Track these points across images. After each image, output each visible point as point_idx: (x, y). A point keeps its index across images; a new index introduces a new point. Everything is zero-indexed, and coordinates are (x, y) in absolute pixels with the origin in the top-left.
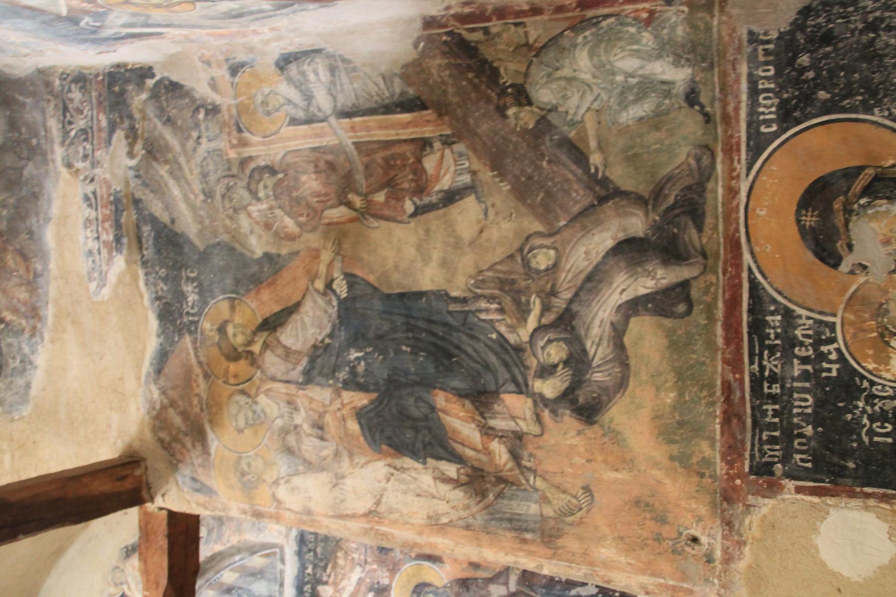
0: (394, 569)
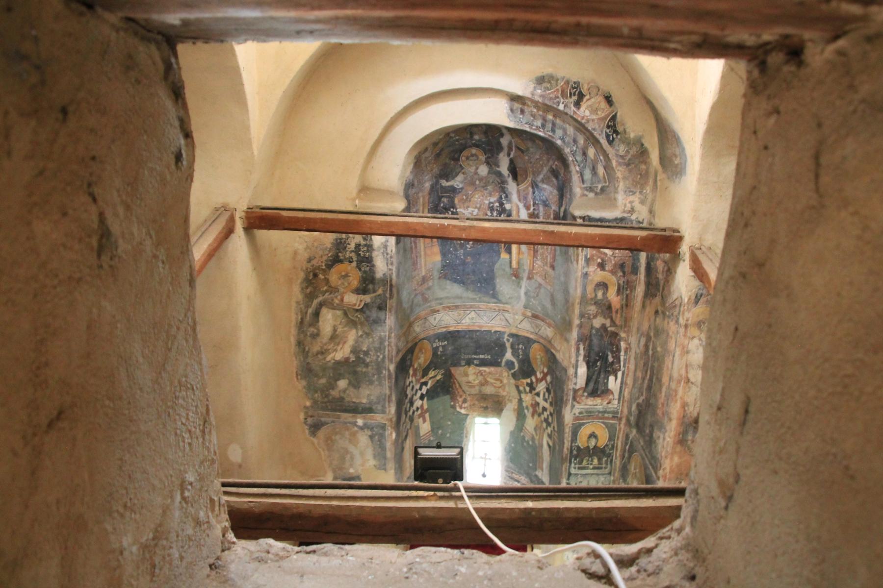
0: (613, 272)
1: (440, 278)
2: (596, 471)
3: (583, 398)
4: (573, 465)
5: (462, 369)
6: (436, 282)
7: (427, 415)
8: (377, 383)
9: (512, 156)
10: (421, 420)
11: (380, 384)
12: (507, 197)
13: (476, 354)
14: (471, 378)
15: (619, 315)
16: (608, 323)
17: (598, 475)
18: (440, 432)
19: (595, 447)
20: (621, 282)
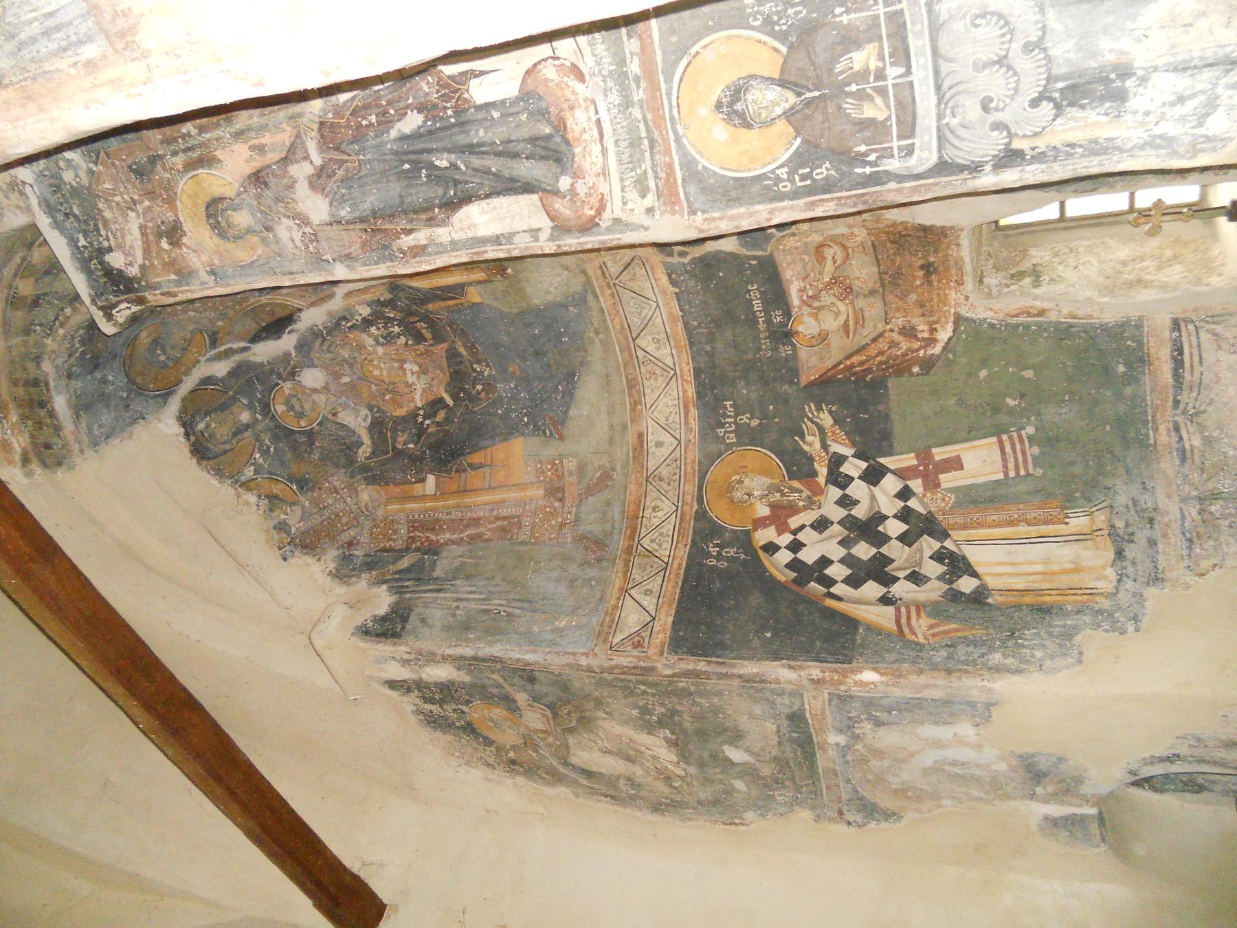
1: (562, 438)
2: (918, 43)
3: (581, 189)
4: (892, 165)
5: (803, 353)
6: (566, 447)
7: (939, 453)
8: (716, 700)
9: (243, 344)
10: (948, 480)
11: (719, 694)
12: (344, 318)
13: (753, 322)
14: (831, 323)
15: (266, 139)
16: (301, 171)
17: (935, 29)
18: (1010, 402)
19: (783, 83)
20: (179, 161)
